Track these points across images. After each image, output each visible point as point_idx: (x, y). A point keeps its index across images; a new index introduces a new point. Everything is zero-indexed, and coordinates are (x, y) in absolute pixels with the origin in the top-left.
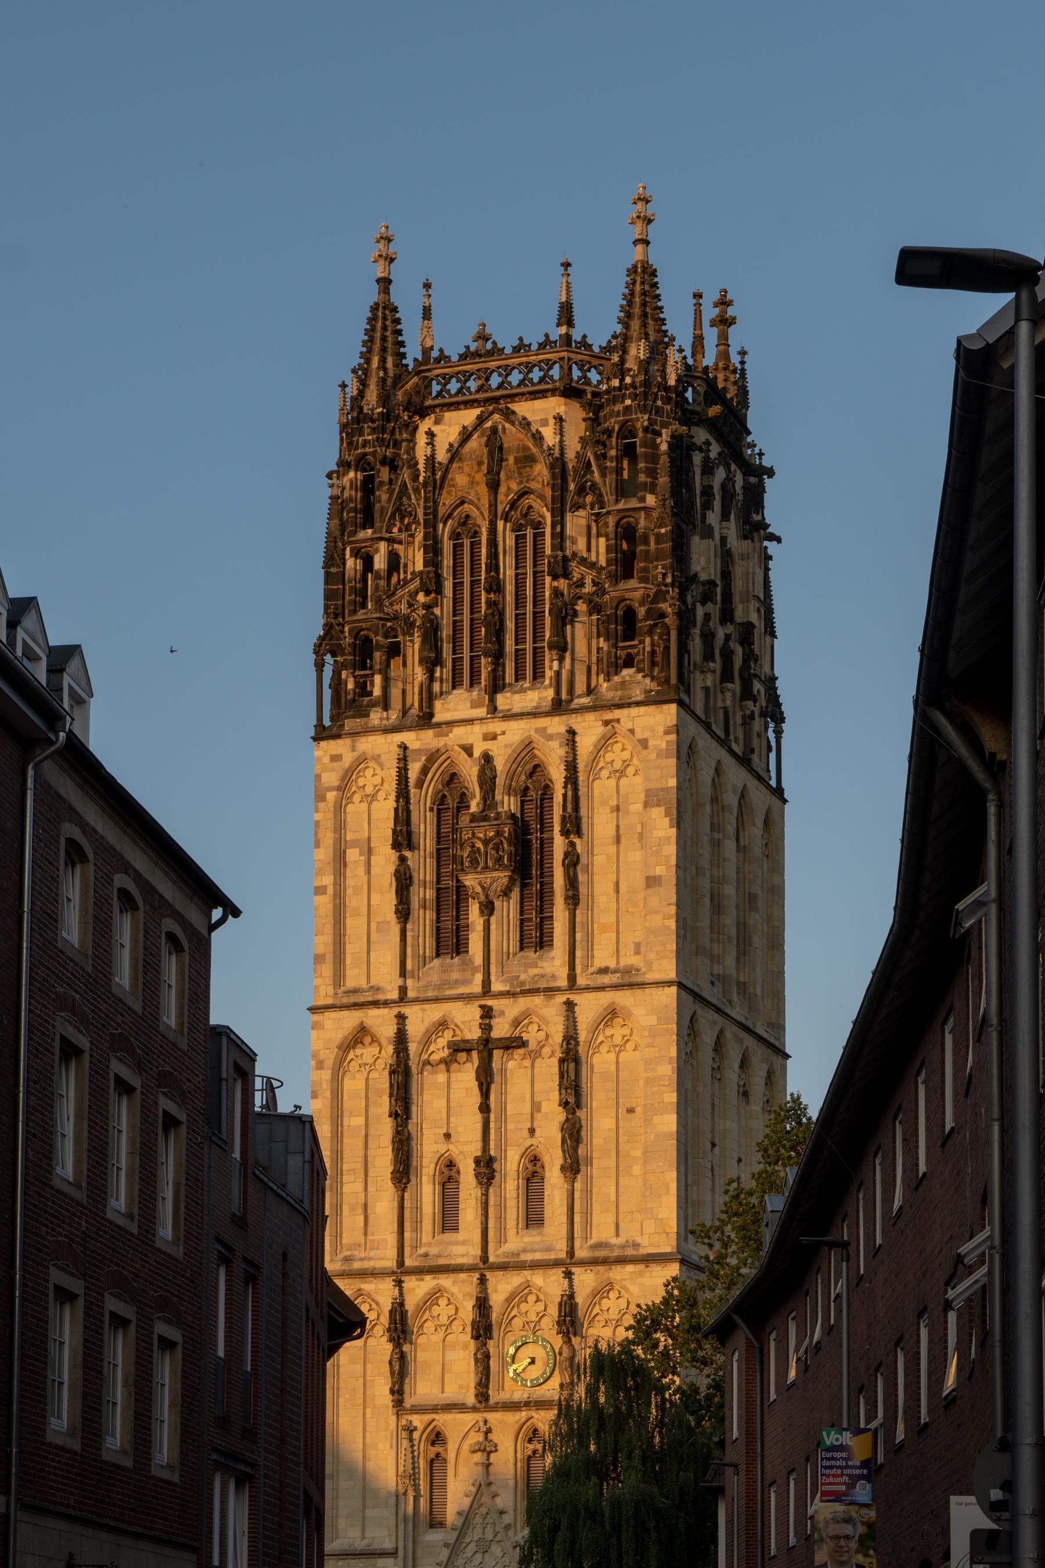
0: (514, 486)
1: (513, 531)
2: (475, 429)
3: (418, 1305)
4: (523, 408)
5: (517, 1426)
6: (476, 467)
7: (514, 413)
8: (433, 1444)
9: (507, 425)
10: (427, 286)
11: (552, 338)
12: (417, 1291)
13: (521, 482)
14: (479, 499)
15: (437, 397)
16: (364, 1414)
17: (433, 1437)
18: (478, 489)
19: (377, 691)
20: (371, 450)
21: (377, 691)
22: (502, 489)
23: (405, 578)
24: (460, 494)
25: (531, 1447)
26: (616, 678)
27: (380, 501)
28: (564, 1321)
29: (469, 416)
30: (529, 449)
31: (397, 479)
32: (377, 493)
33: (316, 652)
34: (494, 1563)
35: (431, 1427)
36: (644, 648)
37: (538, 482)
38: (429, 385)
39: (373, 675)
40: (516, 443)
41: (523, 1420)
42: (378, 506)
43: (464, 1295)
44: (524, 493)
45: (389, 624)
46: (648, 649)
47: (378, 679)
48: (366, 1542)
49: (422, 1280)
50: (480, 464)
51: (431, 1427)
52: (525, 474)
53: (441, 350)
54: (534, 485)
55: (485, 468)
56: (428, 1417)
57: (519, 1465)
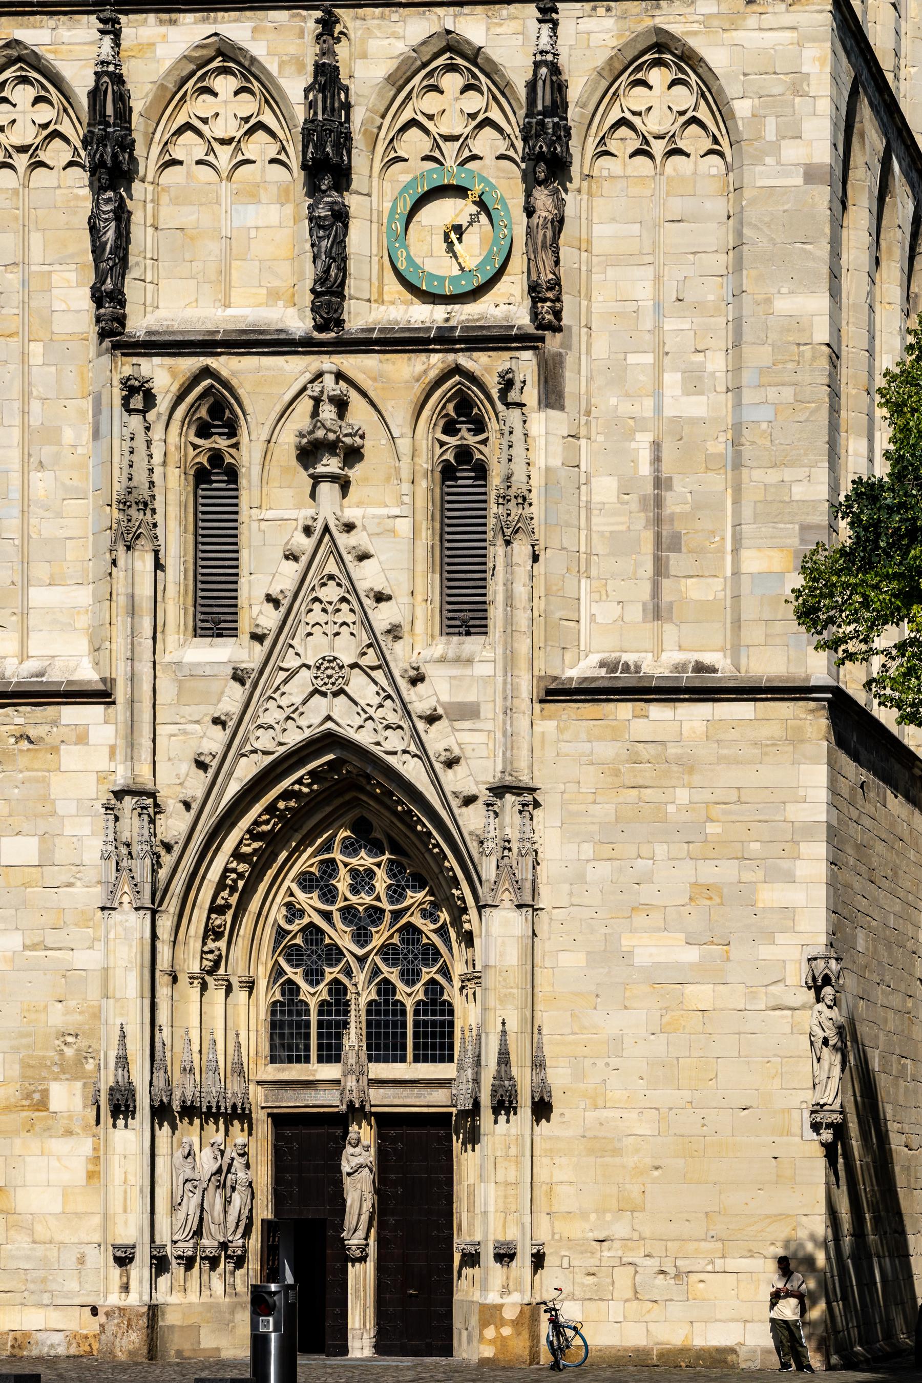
3: (162, 87)
5: (418, 389)
8: (204, 431)
12: (160, 50)
16: (24, 356)
17: (203, 413)
25: (453, 441)
28: (541, 124)
34: (359, 721)
35: (198, 390)
41: (433, 374)
43: (281, 65)
48: (31, 666)
49: (173, 22)
51: (198, 390)
56: (190, 364)
57: (423, 484)
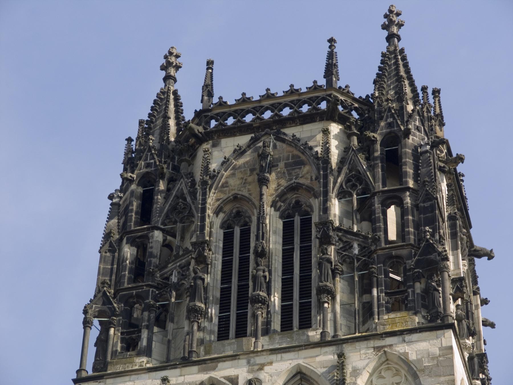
0: (284, 183)
1: (281, 217)
2: (249, 146)
4: (290, 131)
6: (249, 172)
7: (285, 134)
9: (278, 144)
10: (210, 64)
11: (319, 84)
13: (291, 179)
14: (250, 194)
15: (214, 128)
18: (250, 187)
19: (144, 342)
20: (153, 169)
21: (144, 343)
22: (273, 186)
23: (178, 253)
24: (233, 192)
26: (386, 317)
27: (157, 202)
29: (244, 140)
30: (299, 157)
31: (174, 186)
32: (156, 197)
33: (85, 312)
36: (413, 292)
37: (307, 179)
38: (209, 123)
39: (140, 331)
40: (286, 154)
42: (155, 206)
44: (294, 188)
45: (157, 292)
46: (418, 291)
47: (145, 334)
50: (252, 170)
52: (294, 174)
53: (220, 98)
54: (301, 181)
55: (258, 171)
